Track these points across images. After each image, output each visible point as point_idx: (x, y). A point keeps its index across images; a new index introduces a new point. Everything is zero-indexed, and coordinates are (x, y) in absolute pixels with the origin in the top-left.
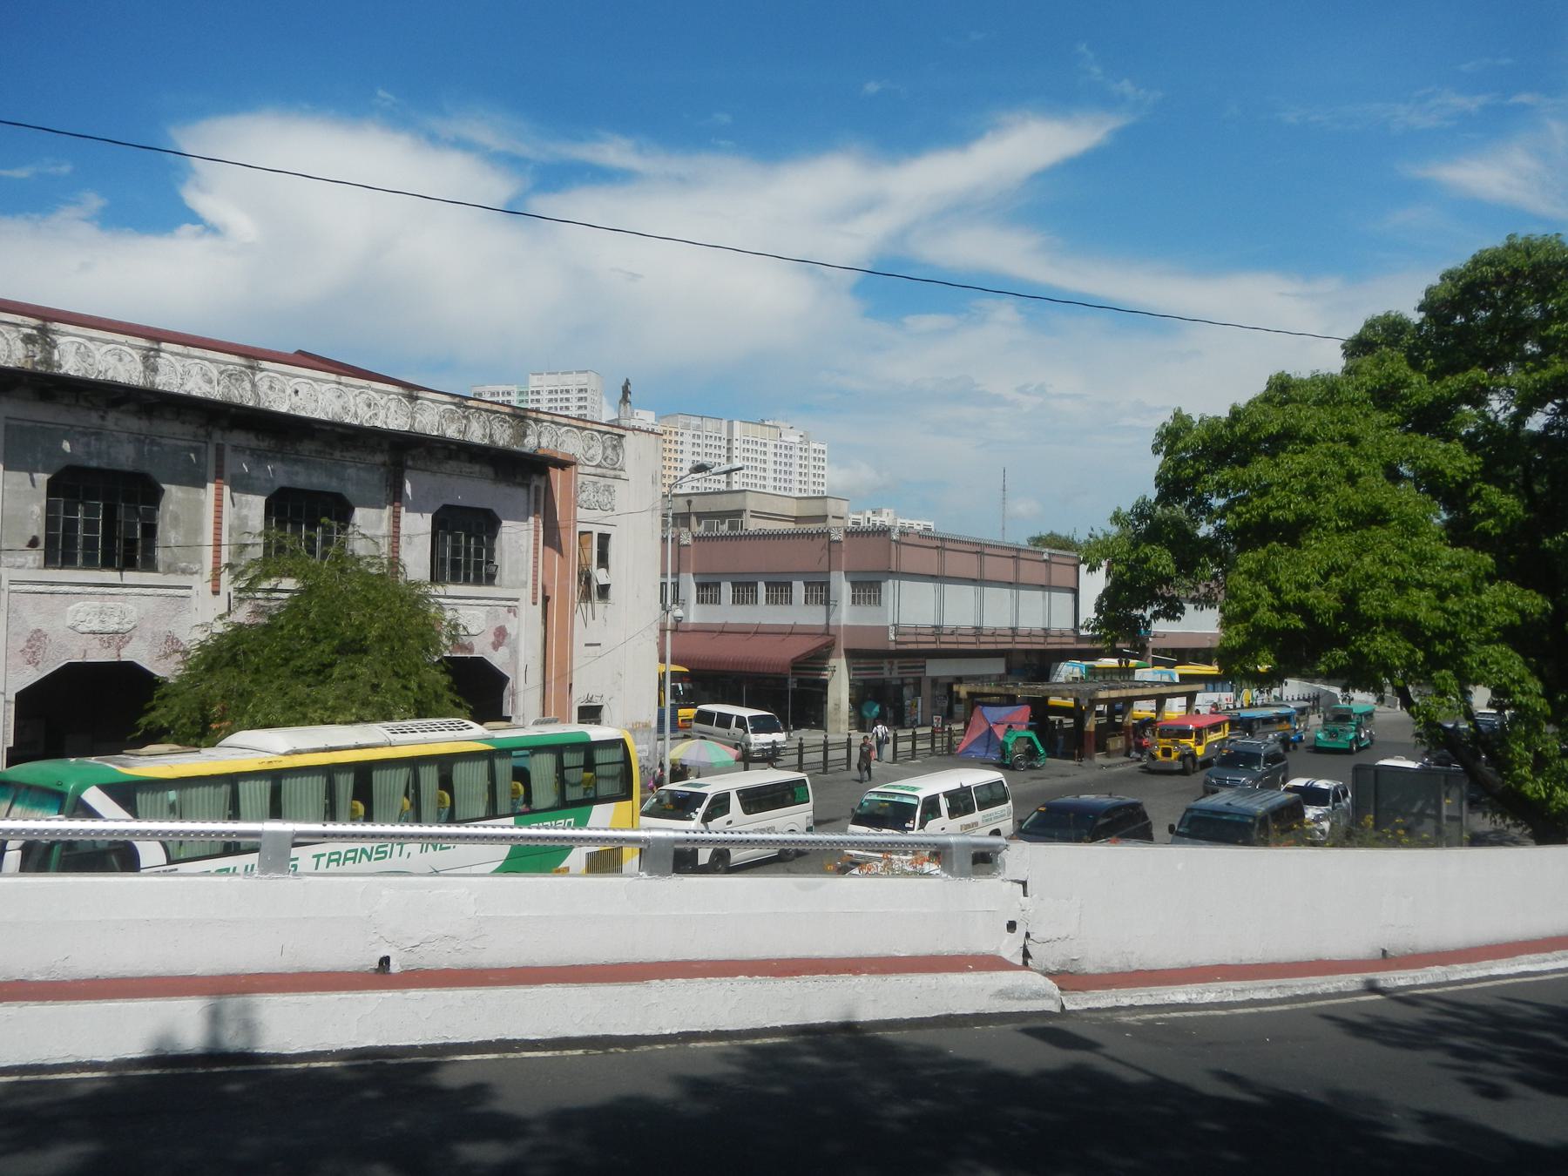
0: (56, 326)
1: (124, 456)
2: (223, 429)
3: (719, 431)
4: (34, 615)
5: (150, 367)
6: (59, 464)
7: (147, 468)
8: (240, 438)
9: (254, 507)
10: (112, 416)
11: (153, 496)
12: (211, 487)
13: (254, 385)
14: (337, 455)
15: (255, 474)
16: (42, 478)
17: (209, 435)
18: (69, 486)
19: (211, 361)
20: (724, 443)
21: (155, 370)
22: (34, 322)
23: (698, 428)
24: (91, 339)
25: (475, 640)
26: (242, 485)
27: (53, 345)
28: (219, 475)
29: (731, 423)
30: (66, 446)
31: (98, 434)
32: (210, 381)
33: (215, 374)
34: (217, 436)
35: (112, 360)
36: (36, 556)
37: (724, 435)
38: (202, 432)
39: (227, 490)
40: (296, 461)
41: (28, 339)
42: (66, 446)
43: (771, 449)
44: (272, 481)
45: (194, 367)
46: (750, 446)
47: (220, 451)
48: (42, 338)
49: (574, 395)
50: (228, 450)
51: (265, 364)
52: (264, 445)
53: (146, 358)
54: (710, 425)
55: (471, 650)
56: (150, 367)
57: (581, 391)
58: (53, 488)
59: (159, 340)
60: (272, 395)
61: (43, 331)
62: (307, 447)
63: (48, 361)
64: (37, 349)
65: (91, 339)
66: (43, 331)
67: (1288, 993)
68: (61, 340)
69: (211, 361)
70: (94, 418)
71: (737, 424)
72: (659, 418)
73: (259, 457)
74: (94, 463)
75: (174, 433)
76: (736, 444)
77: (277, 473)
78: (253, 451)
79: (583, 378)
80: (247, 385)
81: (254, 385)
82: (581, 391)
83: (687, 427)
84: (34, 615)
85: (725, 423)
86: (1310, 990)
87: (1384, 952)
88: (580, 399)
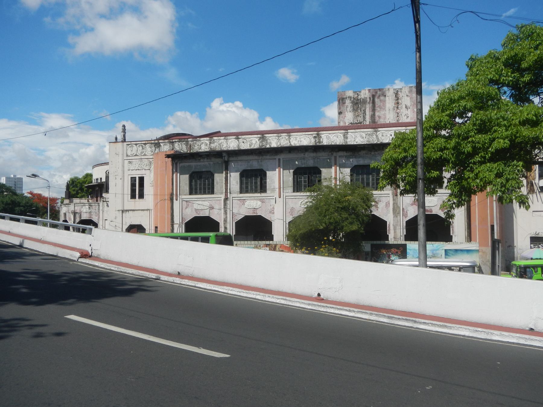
0: (321, 132)
1: (310, 163)
2: (336, 152)
4: (291, 204)
5: (345, 137)
6: (295, 167)
7: (316, 165)
8: (341, 153)
9: (347, 171)
10: (307, 154)
11: (320, 172)
12: (333, 168)
13: (377, 136)
14: (373, 153)
15: (347, 162)
16: (292, 171)
17: (332, 154)
18: (298, 172)
19: (363, 132)
21: (347, 138)
22: (315, 133)
24: (330, 134)
25: (433, 209)
26: (342, 166)
27: (321, 137)
28: (335, 164)
30: (297, 163)
31: (304, 159)
32: (363, 138)
33: (364, 135)
34: (335, 154)
35: (335, 138)
36: (291, 189)
38: (330, 154)
39: (338, 168)
40: (359, 157)
41: (315, 137)
42: (297, 163)
44: (352, 164)
45: (358, 135)
47: (335, 157)
48: (318, 136)
50: (338, 157)
51: (380, 129)
52: (348, 154)
53: (344, 135)
55: (431, 211)
56: (345, 137)
58: (295, 173)
59: (347, 130)
60: (383, 138)
61: (318, 134)
62: (362, 153)
63: (319, 142)
64: (317, 139)
65: (330, 134)
66: (318, 134)
67: (119, 270)
68: (322, 136)
69: (363, 132)
70: (302, 155)
73: (348, 158)
74: (303, 166)
75: (323, 155)
77: (354, 161)
78: (346, 156)
80: (375, 136)
81: (377, 136)
84: (291, 204)
86: (125, 271)
87: (179, 273)
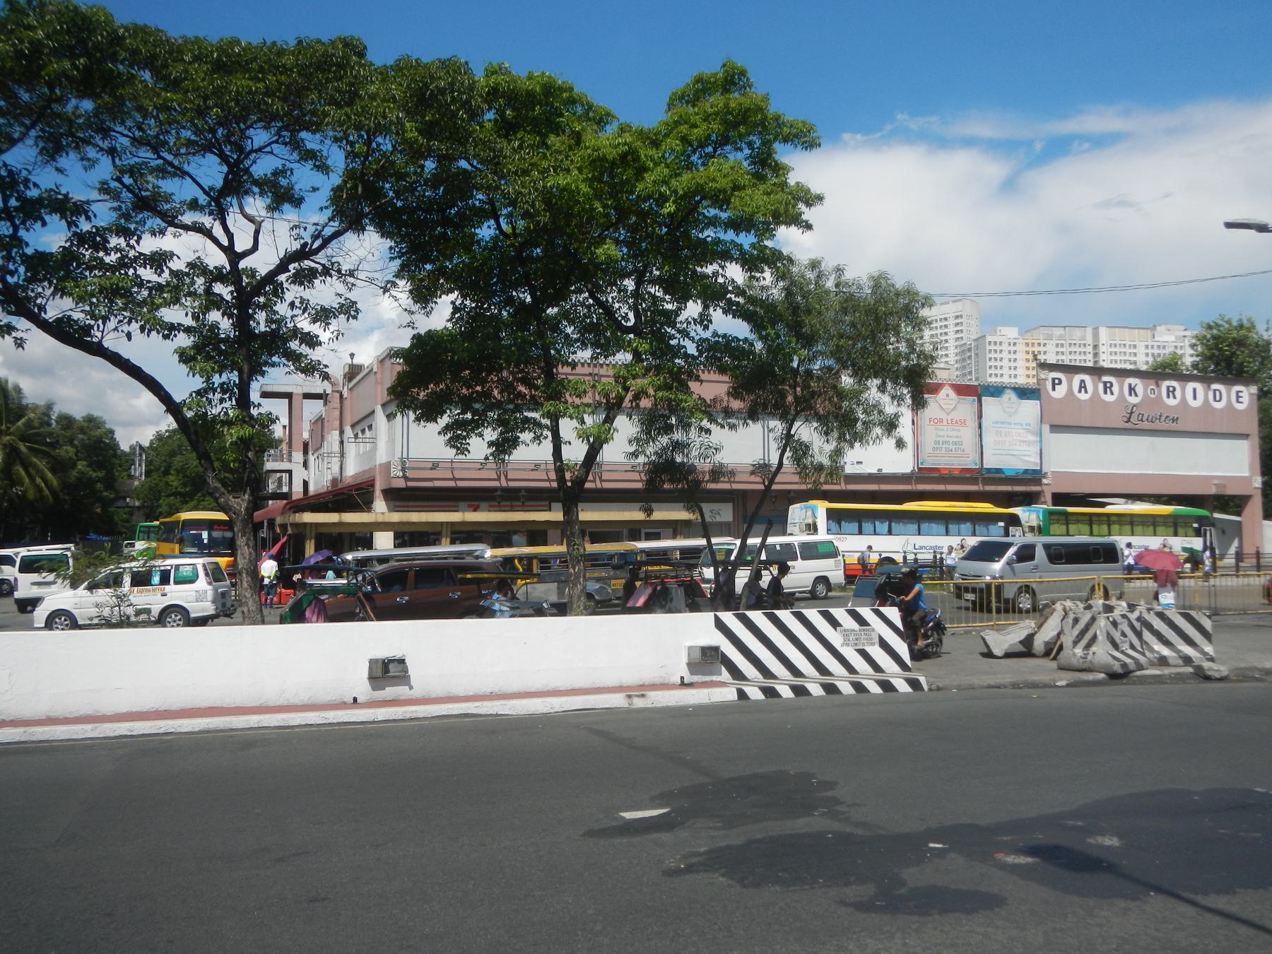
3: (1083, 338)
20: (1090, 349)
23: (1060, 338)
29: (1096, 330)
37: (1089, 340)
43: (1141, 350)
46: (1118, 350)
49: (951, 322)
54: (1078, 333)
57: (957, 317)
71: (1103, 332)
72: (1024, 332)
76: (1102, 349)
79: (959, 306)
82: (957, 317)
83: (1050, 337)
85: (1089, 331)
88: (957, 324)
